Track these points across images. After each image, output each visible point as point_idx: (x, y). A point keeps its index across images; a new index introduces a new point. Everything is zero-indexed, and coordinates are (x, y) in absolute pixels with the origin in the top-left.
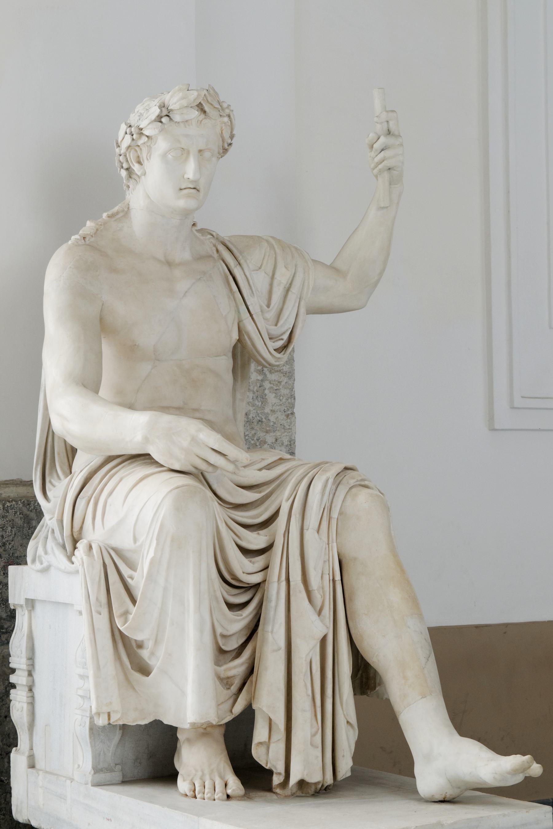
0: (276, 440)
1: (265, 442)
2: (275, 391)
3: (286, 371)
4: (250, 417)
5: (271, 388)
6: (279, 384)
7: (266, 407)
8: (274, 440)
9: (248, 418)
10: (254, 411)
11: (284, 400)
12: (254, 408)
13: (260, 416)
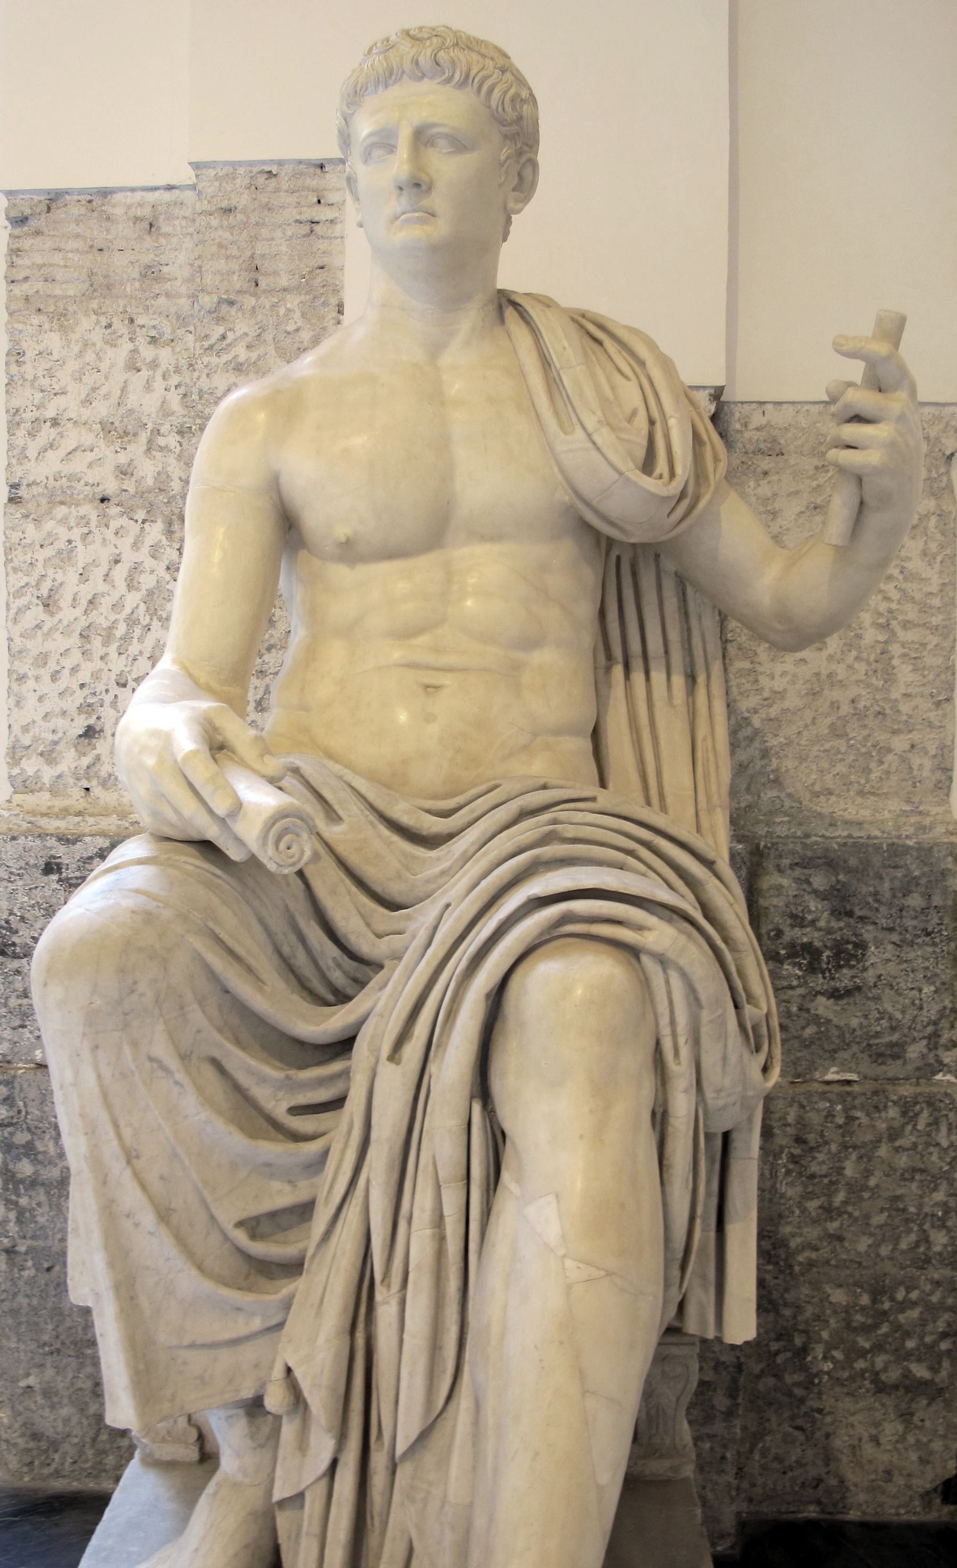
0: (913, 746)
1: (889, 750)
2: (913, 661)
3: (937, 626)
4: (861, 705)
5: (904, 655)
6: (921, 648)
7: (893, 690)
8: (908, 747)
9: (855, 708)
10: (868, 696)
11: (931, 677)
12: (868, 690)
13: (881, 703)
